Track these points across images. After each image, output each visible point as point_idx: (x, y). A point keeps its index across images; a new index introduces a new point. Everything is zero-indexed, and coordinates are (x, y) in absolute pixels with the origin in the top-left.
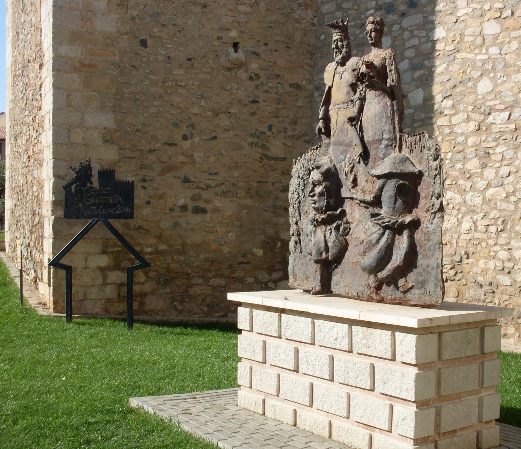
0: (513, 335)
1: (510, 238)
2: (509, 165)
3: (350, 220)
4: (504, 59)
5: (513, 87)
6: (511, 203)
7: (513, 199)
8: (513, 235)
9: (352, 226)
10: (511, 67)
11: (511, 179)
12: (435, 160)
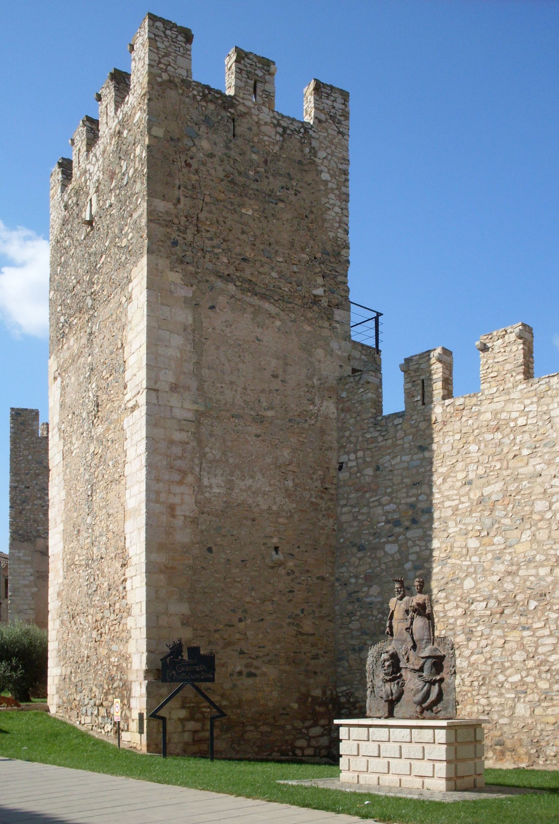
0: (492, 758)
1: (488, 690)
2: (486, 639)
3: (405, 679)
4: (483, 566)
5: (489, 585)
6: (488, 665)
7: (489, 662)
8: (490, 687)
9: (406, 682)
10: (487, 571)
11: (488, 648)
12: (452, 650)
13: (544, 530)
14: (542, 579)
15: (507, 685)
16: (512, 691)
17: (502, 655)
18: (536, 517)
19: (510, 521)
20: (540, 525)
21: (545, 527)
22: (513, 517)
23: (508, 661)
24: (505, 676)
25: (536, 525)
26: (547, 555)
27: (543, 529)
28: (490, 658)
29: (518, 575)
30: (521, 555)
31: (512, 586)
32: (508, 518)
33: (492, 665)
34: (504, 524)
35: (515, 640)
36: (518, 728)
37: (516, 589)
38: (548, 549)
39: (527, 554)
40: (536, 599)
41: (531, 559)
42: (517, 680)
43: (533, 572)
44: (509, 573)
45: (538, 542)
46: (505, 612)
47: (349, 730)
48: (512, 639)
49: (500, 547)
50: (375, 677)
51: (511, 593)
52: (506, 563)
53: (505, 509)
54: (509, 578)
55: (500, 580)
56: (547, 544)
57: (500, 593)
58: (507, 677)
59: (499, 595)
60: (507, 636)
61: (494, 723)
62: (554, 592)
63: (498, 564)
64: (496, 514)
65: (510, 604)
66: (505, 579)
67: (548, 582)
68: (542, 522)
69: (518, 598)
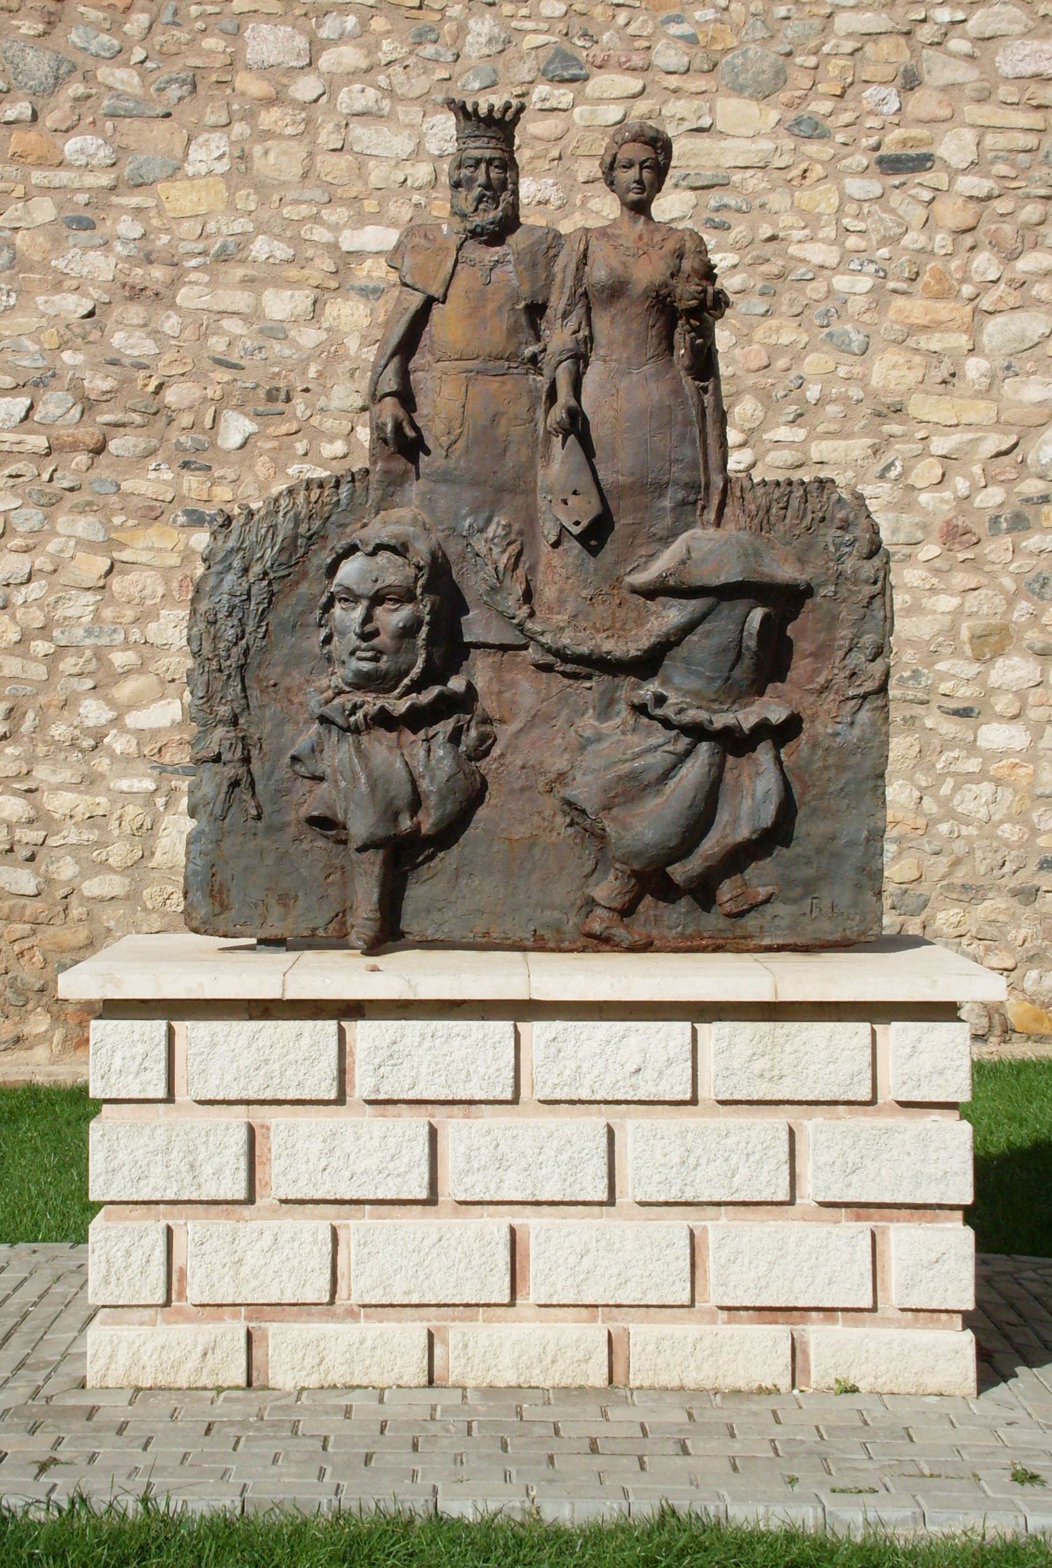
0: (44, 1038)
1: (31, 759)
2: (27, 550)
3: (494, 712)
4: (11, 246)
5: (40, 329)
6: (35, 659)
7: (41, 647)
8: (41, 750)
9: (504, 733)
10: (31, 269)
11: (36, 589)
12: (870, 555)
13: (285, 145)
14: (276, 332)
15: (119, 743)
16: (142, 766)
17: (97, 617)
18: (252, 86)
19: (136, 80)
20: (268, 118)
21: (290, 131)
22: (149, 65)
23: (126, 645)
24: (111, 703)
25: (249, 117)
26: (297, 241)
27: (281, 137)
28: (44, 631)
29: (173, 306)
30: (186, 225)
31: (149, 347)
32: (126, 64)
33: (52, 660)
34: (111, 88)
35: (157, 563)
36: (165, 914)
37: (168, 357)
38: (303, 221)
39: (211, 227)
40: (250, 408)
41: (232, 248)
42: (166, 722)
43: (241, 300)
44: (136, 293)
45: (261, 188)
46: (112, 446)
47: (171, 1033)
48: (144, 557)
49: (90, 180)
50: (254, 693)
51: (142, 374)
52: (118, 247)
53: (114, 28)
54: (135, 313)
55: (91, 314)
56: (297, 202)
57: (95, 367)
58: (121, 710)
59: (88, 374)
60: (122, 546)
61: (62, 892)
62: (326, 390)
63: (85, 249)
64: (73, 37)
65: (137, 418)
66: (116, 312)
67: (298, 347)
68: (275, 112)
69: (170, 396)
